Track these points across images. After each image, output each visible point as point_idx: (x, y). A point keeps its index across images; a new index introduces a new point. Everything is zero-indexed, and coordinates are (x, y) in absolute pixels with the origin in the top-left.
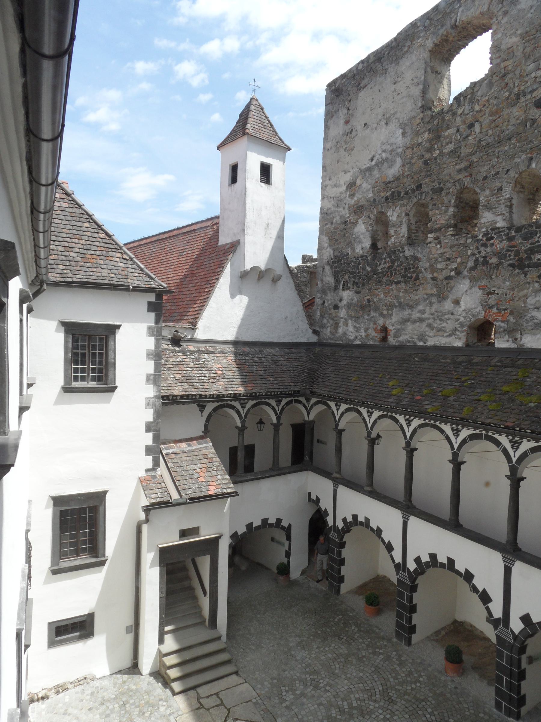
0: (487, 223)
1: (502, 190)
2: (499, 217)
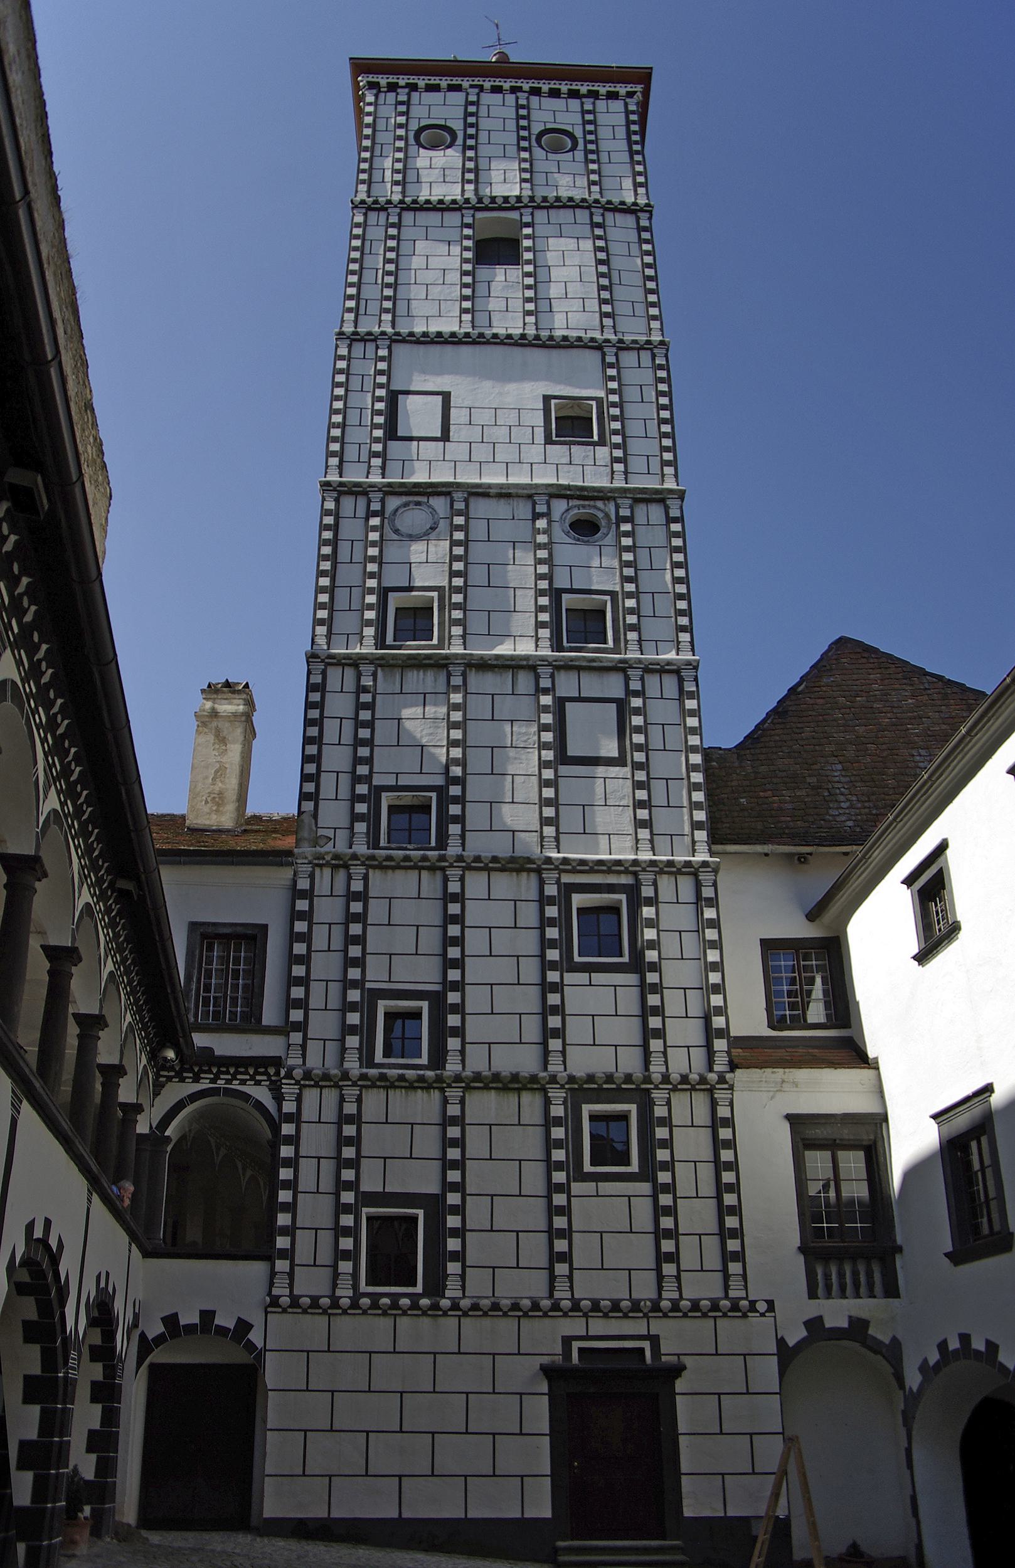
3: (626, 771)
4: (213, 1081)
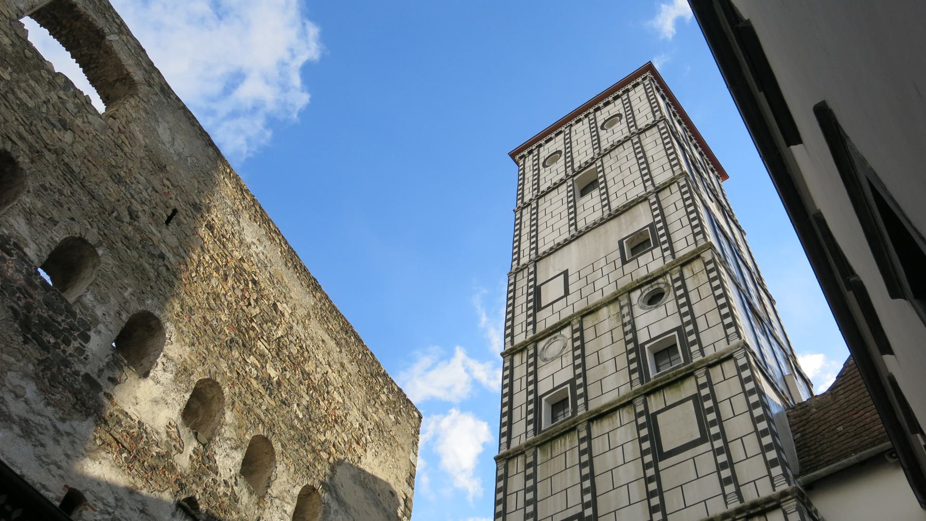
0: (15, 230)
1: (55, 225)
2: (34, 244)
3: (706, 446)
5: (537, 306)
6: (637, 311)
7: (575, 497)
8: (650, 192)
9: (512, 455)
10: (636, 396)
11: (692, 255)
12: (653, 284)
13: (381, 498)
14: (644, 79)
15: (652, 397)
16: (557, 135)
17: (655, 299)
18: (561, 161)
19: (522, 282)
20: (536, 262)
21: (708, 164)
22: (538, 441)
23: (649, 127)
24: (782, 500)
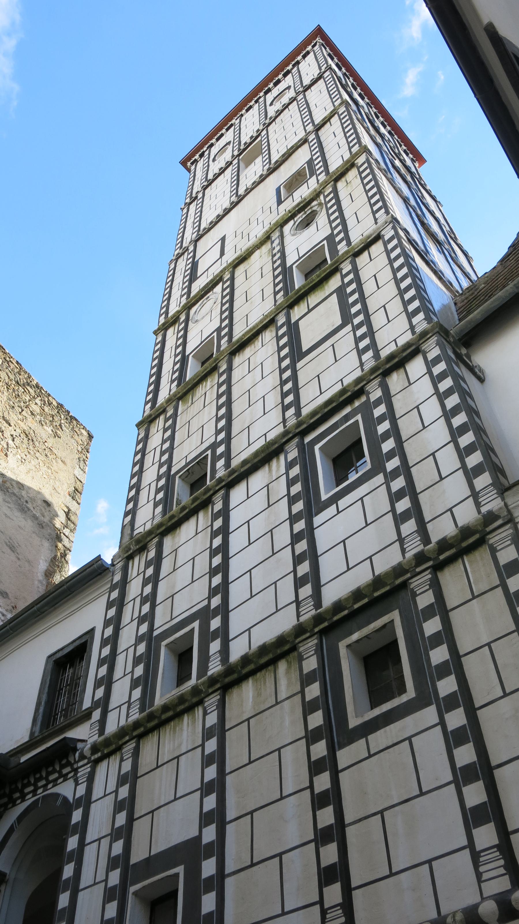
4: (34, 792)
5: (193, 276)
6: (288, 239)
7: (210, 431)
8: (309, 132)
9: (153, 416)
10: (278, 311)
11: (345, 166)
12: (306, 210)
13: (30, 505)
14: (314, 46)
15: (296, 308)
16: (227, 130)
17: (307, 223)
18: (230, 148)
19: (182, 264)
20: (196, 241)
21: (401, 146)
22: (179, 393)
23: (314, 82)
24: (421, 342)
